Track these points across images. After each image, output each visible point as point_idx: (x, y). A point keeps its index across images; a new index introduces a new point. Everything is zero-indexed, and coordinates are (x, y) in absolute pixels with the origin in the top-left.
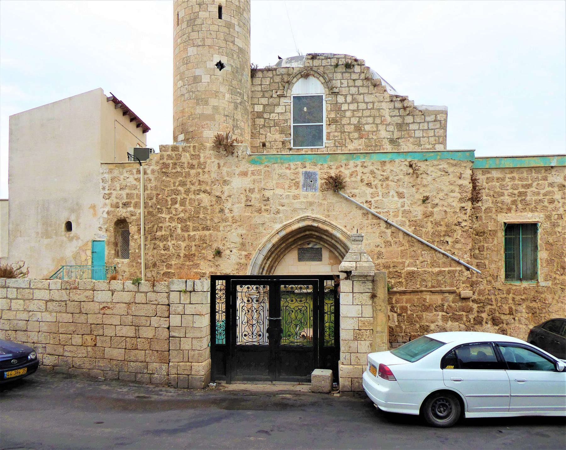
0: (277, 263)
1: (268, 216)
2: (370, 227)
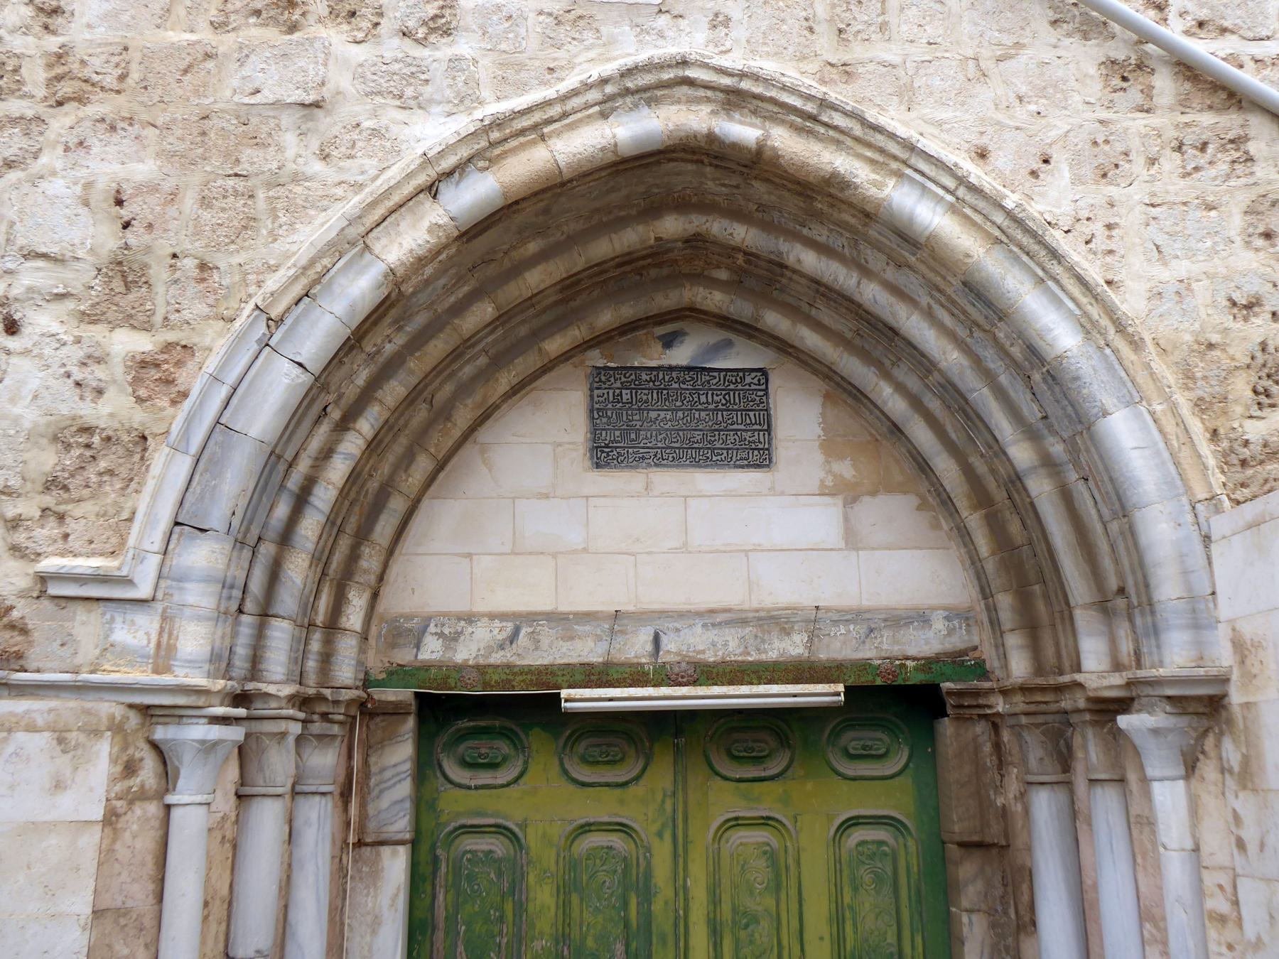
0: (423, 465)
1: (360, 53)
2: (1170, 162)
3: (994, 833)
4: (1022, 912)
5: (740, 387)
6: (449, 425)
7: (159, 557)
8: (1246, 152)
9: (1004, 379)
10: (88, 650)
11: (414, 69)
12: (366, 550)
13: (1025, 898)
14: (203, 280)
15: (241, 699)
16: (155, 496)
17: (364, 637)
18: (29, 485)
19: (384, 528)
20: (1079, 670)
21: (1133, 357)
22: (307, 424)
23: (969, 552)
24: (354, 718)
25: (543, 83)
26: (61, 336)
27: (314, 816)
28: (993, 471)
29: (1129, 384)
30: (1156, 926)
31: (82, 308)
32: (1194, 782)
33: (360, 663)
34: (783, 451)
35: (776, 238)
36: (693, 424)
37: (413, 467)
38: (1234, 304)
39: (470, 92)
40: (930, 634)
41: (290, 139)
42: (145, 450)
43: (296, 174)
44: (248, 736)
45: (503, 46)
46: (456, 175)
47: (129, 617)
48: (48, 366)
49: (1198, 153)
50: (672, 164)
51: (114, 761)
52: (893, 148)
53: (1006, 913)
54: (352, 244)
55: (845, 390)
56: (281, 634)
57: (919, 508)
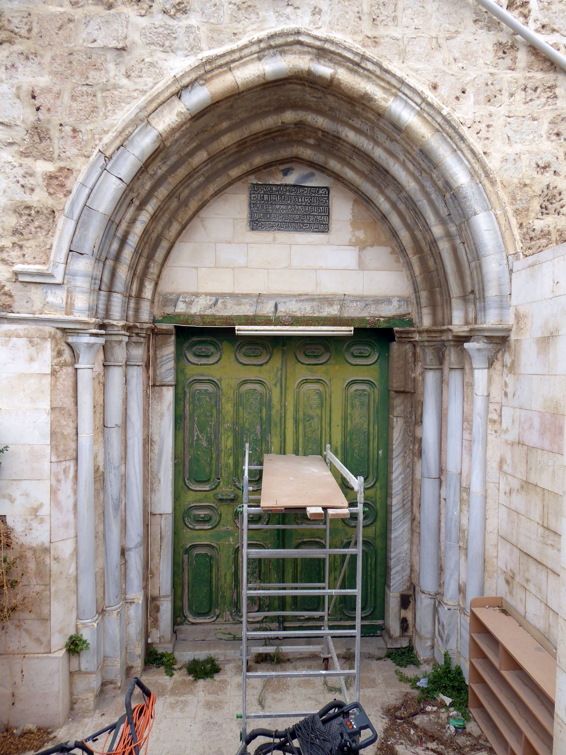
0: (176, 227)
1: (143, 22)
2: (520, 96)
3: (409, 388)
4: (417, 418)
5: (317, 195)
6: (187, 209)
7: (64, 265)
8: (555, 93)
9: (433, 196)
10: (38, 305)
11: (169, 31)
12: (152, 264)
13: (419, 412)
14: (75, 137)
15: (102, 326)
16: (60, 238)
17: (152, 302)
18: (6, 232)
19: (159, 255)
20: (451, 324)
21: (491, 189)
22: (124, 207)
23: (410, 273)
24: (150, 335)
25: (231, 41)
26: (13, 163)
27: (135, 374)
28: (425, 238)
29: (488, 201)
30: (469, 423)
31: (21, 149)
32: (491, 370)
33: (151, 313)
34: (334, 225)
35: (337, 124)
36: (295, 212)
37: (172, 227)
38: (538, 166)
39: (196, 44)
40: (391, 307)
41: (111, 66)
42: (54, 217)
43: (115, 84)
44: (106, 341)
45: (212, 21)
46: (190, 87)
47: (53, 291)
48: (9, 177)
49: (532, 92)
50: (290, 86)
51: (53, 350)
52: (394, 82)
53: (411, 418)
54: (142, 121)
55: (363, 198)
56: (117, 300)
57: (391, 253)
